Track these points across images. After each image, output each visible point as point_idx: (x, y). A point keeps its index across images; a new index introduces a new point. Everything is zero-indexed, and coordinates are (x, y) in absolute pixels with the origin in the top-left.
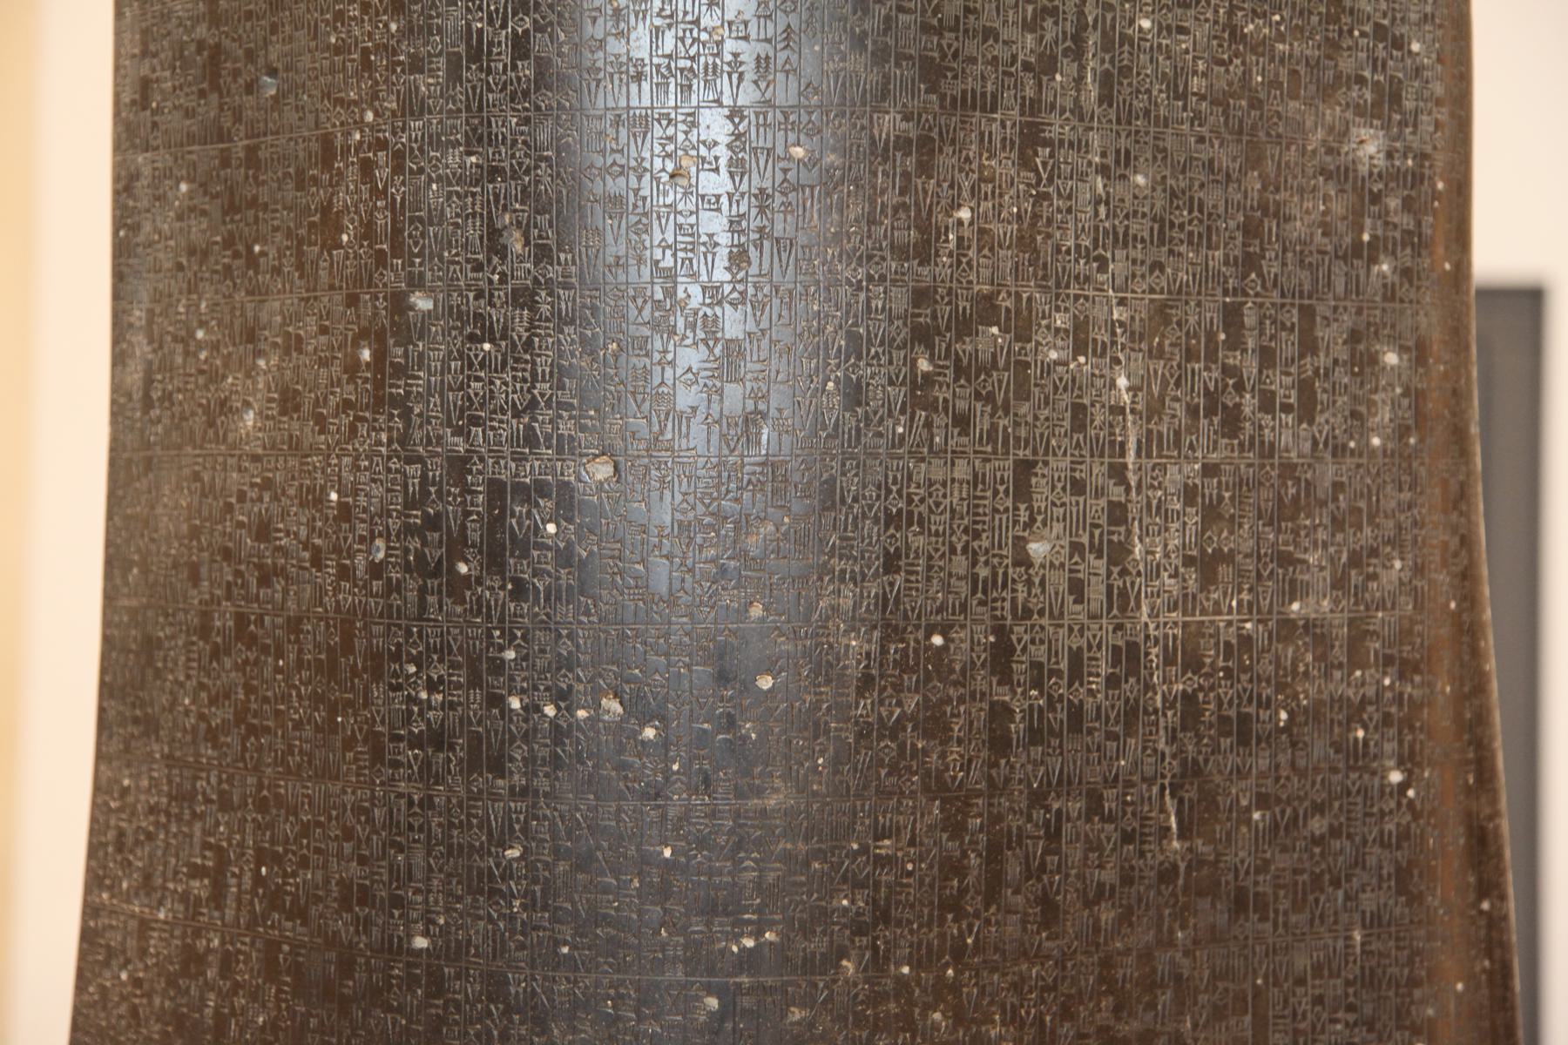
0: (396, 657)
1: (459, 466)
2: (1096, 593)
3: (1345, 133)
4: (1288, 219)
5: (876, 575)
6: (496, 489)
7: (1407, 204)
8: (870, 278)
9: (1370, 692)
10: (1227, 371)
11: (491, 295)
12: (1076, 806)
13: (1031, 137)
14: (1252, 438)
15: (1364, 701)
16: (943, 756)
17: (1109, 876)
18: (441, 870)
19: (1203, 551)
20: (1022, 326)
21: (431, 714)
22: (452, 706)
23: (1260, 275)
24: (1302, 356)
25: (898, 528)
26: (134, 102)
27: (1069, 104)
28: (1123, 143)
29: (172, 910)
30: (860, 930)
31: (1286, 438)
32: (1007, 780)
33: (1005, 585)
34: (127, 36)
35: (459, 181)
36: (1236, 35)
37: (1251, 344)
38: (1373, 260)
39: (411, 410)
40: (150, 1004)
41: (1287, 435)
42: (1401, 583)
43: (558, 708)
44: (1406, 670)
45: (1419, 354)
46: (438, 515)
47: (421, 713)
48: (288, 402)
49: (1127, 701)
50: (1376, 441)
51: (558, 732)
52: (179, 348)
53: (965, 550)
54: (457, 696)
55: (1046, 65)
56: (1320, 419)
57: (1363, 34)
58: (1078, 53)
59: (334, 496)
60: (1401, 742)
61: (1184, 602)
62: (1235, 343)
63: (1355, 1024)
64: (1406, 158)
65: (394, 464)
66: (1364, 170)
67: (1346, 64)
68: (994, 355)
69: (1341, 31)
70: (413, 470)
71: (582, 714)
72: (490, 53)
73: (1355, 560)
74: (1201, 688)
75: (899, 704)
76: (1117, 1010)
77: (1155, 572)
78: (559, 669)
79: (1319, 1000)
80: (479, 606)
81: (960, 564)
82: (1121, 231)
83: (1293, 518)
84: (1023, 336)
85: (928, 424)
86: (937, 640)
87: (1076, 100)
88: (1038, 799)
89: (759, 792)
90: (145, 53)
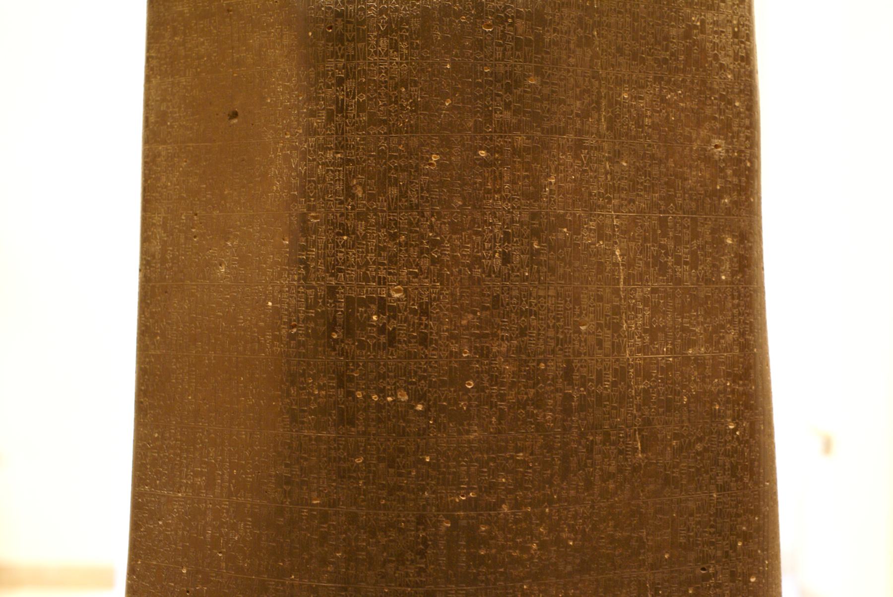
0: (303, 375)
1: (332, 291)
2: (607, 345)
3: (709, 142)
4: (686, 179)
5: (517, 337)
6: (349, 300)
7: (735, 173)
8: (513, 208)
9: (721, 387)
10: (661, 247)
11: (348, 215)
12: (599, 438)
13: (579, 145)
14: (672, 276)
15: (719, 392)
16: (545, 416)
17: (612, 469)
18: (325, 468)
19: (651, 326)
20: (576, 229)
21: (320, 400)
22: (330, 397)
23: (675, 204)
24: (692, 240)
25: (526, 317)
26: (156, 122)
27: (594, 131)
28: (617, 147)
29: (185, 492)
30: (509, 492)
31: (686, 276)
32: (571, 427)
33: (570, 342)
34: (153, 92)
35: (333, 164)
36: (663, 100)
37: (671, 234)
38: (721, 198)
39: (309, 265)
40: (176, 534)
42: (734, 341)
43: (379, 397)
44: (735, 378)
46: (323, 311)
47: (315, 399)
49: (620, 393)
50: (723, 277)
51: (379, 407)
52: (182, 236)
53: (553, 326)
54: (332, 392)
55: (585, 115)
56: (700, 268)
57: (715, 99)
58: (598, 109)
59: (270, 304)
60: (734, 410)
61: (643, 349)
62: (665, 235)
63: (714, 533)
64: (734, 152)
65: (301, 290)
66: (716, 157)
67: (708, 112)
68: (565, 241)
69: (706, 98)
70: (309, 291)
71: (389, 399)
72: (347, 109)
73: (716, 330)
74: (651, 387)
75: (526, 394)
76: (615, 526)
77: (631, 336)
78: (379, 379)
79: (699, 523)
80: (343, 353)
81: (551, 333)
82: (616, 185)
83: (689, 312)
84: (577, 232)
85: (538, 271)
86: (542, 366)
87: (598, 129)
88: (582, 435)
89: (468, 432)
90: (164, 100)
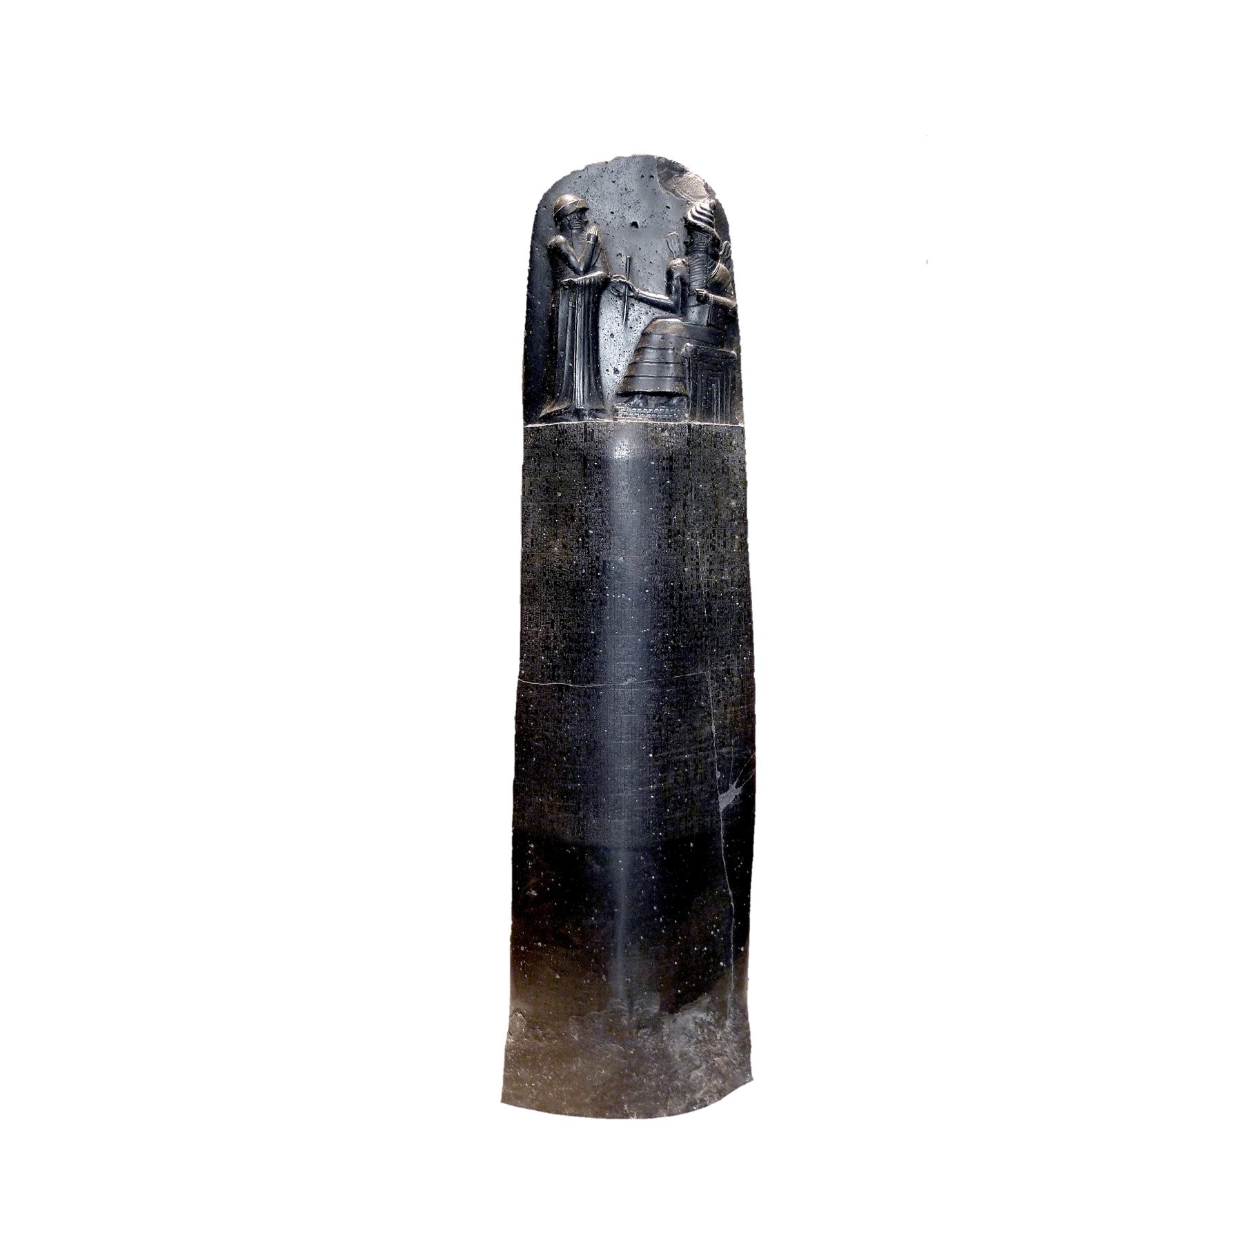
1: (598, 558)
13: (685, 505)
41: (723, 551)
45: (741, 536)
48: (564, 546)
